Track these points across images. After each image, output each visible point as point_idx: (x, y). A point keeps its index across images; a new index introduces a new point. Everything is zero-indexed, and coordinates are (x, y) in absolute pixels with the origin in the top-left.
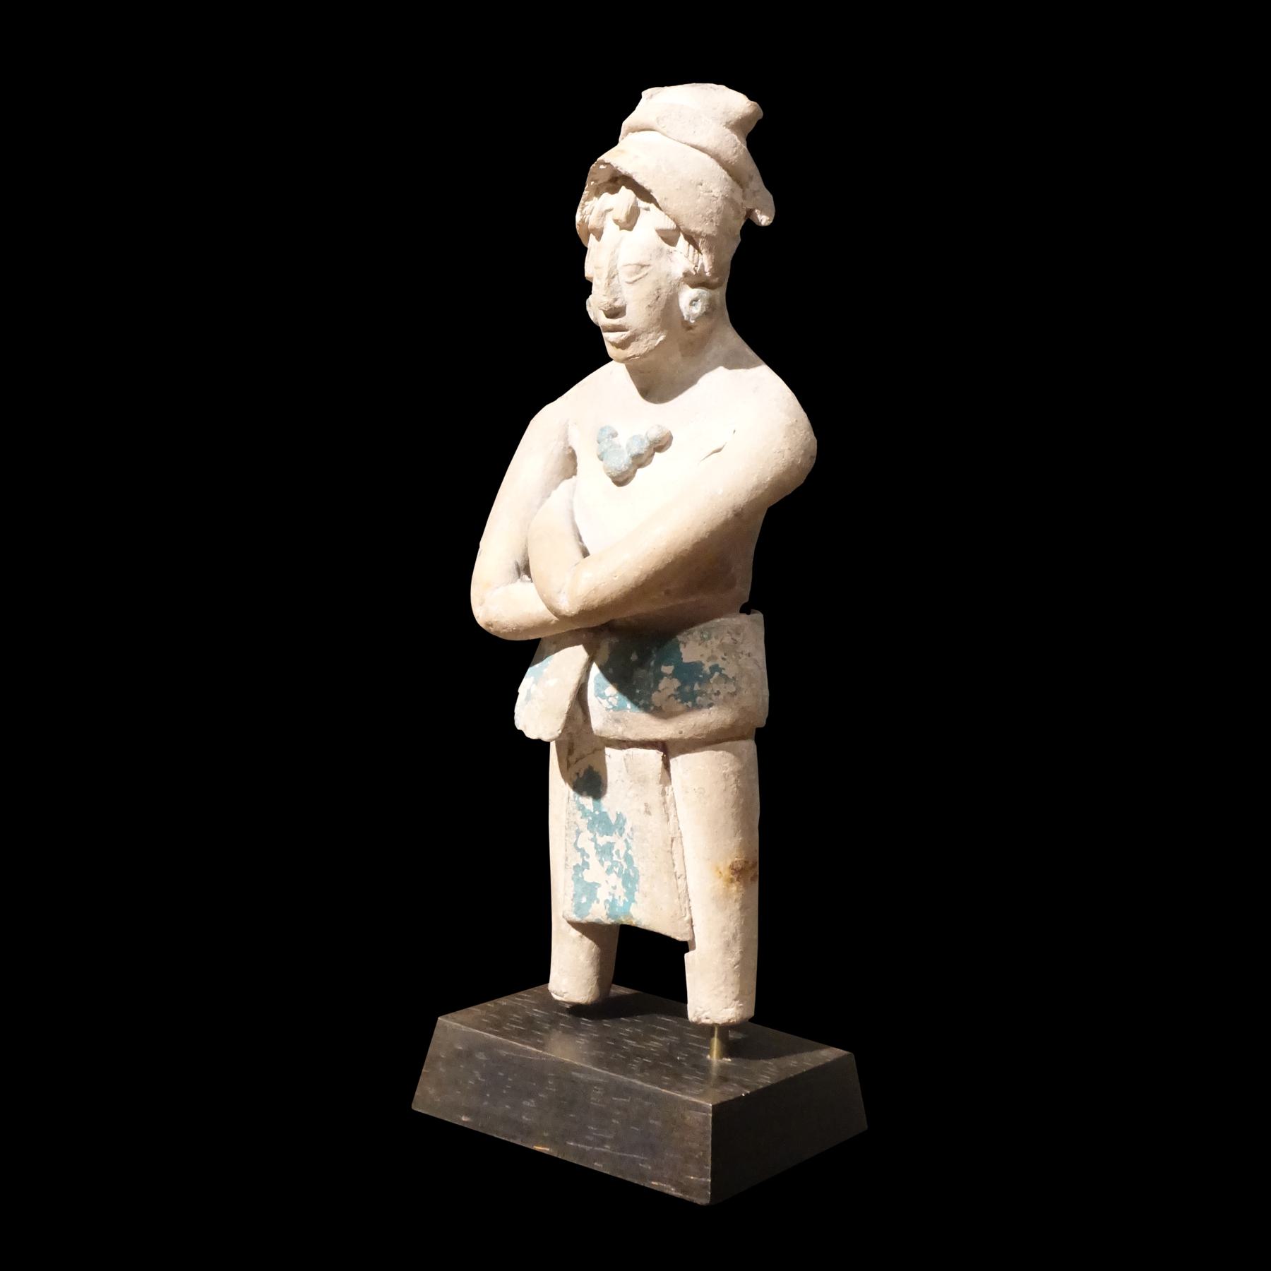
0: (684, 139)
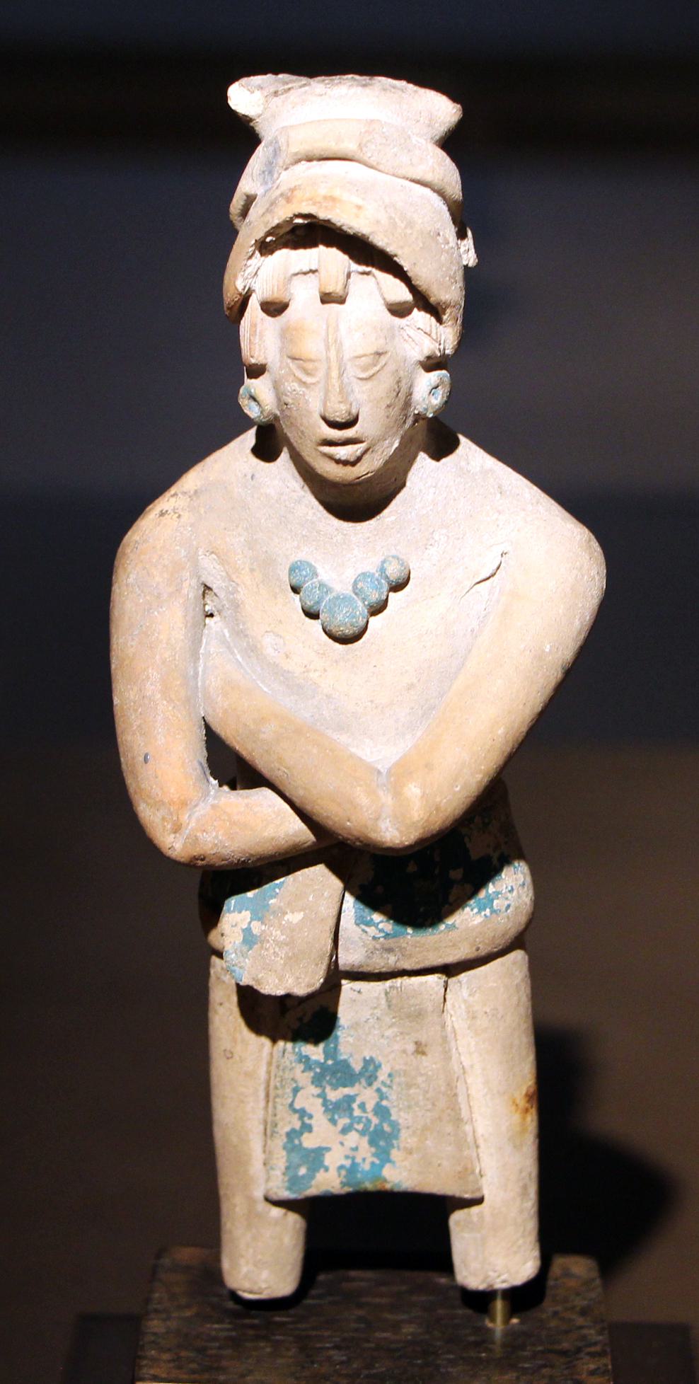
0: (402, 172)
